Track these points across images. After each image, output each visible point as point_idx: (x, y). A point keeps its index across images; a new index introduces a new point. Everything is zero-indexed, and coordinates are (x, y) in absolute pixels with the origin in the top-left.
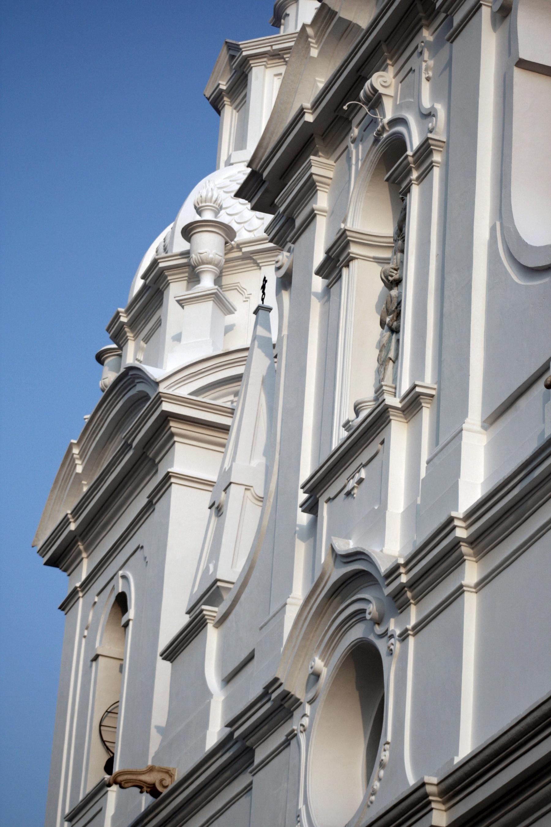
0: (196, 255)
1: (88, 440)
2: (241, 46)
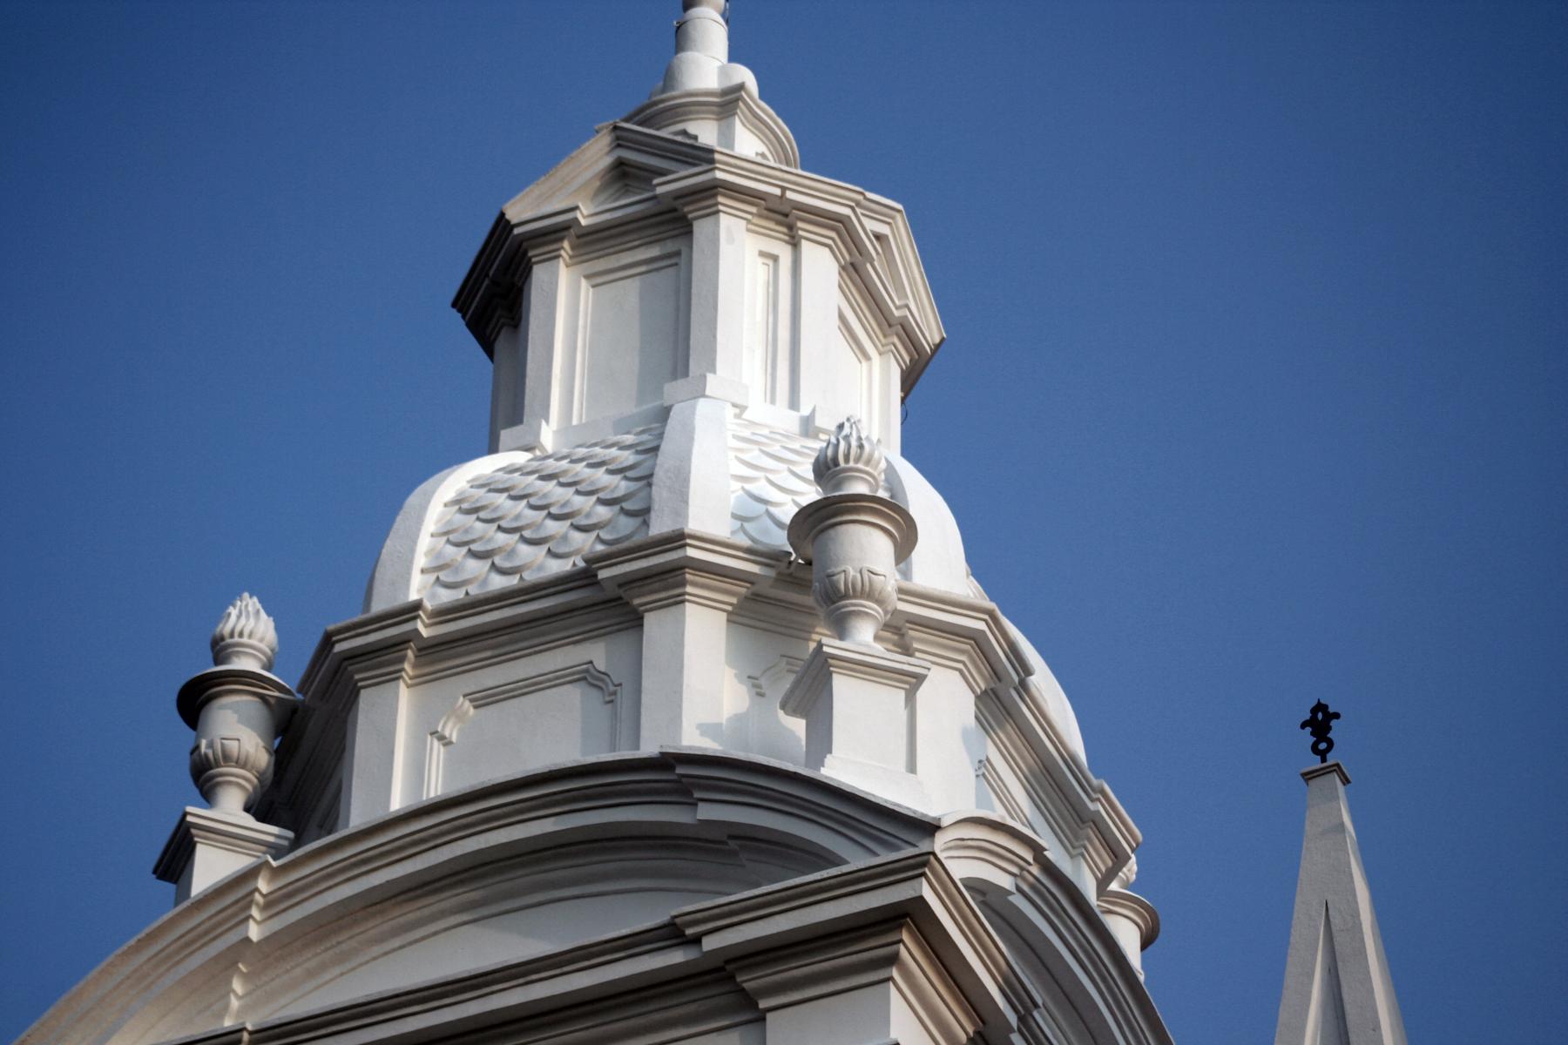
0: (853, 568)
1: (324, 872)
2: (717, 156)
